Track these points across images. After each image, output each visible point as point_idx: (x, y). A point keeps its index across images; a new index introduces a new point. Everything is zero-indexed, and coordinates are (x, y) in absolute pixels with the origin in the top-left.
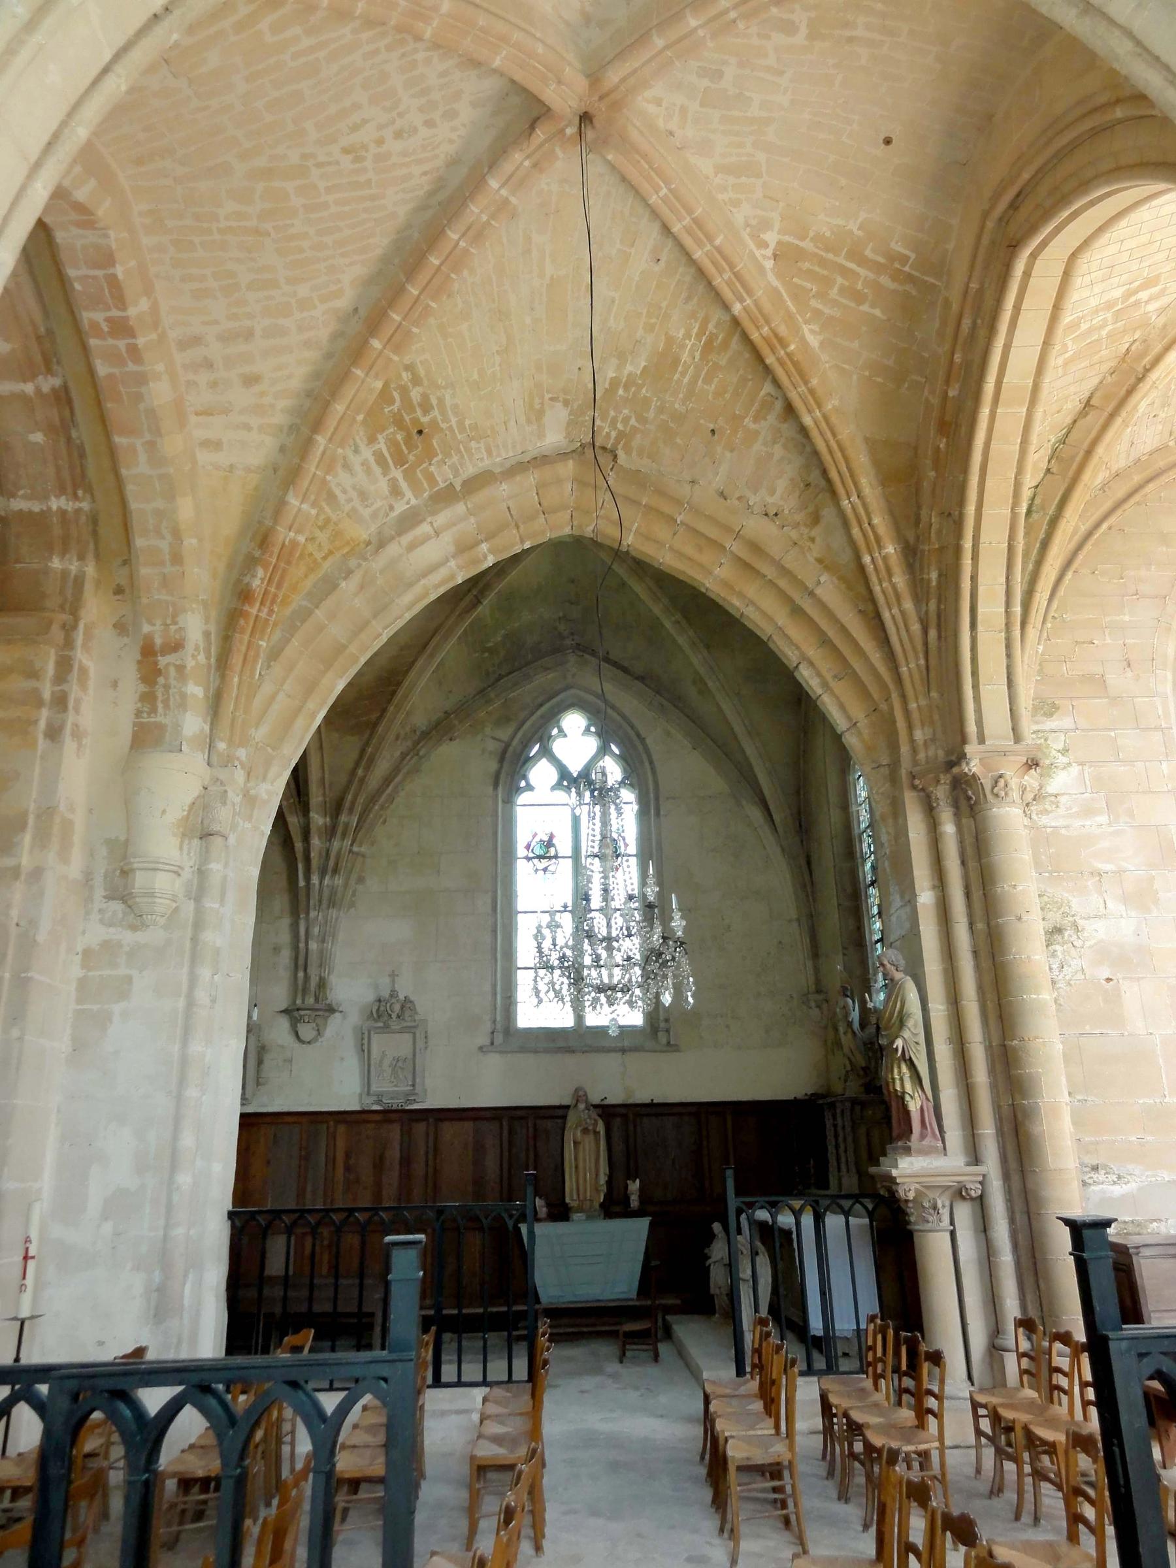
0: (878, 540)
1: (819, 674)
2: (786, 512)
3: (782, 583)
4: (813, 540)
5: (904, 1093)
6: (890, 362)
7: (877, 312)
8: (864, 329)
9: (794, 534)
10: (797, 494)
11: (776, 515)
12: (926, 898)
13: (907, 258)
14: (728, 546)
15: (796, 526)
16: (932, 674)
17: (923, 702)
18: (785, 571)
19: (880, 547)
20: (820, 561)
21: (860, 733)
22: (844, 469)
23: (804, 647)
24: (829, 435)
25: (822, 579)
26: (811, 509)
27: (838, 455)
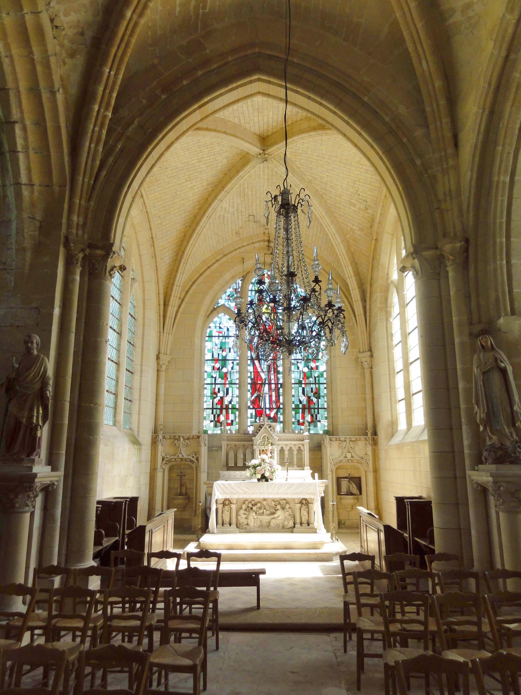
0: (108, 104)
1: (26, 139)
2: (64, 33)
3: (39, 69)
4: (65, 63)
5: (37, 425)
6: (159, 33)
7: (178, 9)
8: (168, 8)
9: (58, 48)
10: (75, 31)
11: (57, 27)
12: (57, 311)
13: (204, 7)
14: (25, 11)
15: (62, 46)
16: (95, 193)
17: (83, 202)
18: (47, 66)
19: (107, 109)
20: (62, 80)
21: (32, 192)
22: (119, 54)
23: (26, 116)
24: (128, 32)
25: (61, 91)
26: (74, 47)
27: (123, 46)
